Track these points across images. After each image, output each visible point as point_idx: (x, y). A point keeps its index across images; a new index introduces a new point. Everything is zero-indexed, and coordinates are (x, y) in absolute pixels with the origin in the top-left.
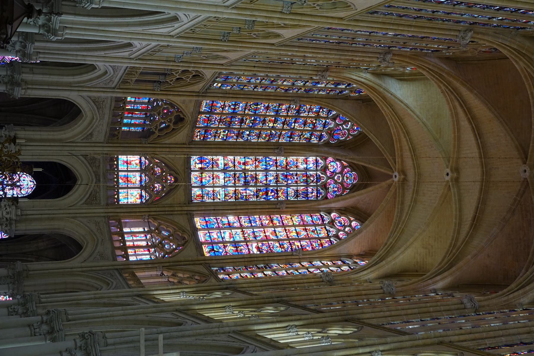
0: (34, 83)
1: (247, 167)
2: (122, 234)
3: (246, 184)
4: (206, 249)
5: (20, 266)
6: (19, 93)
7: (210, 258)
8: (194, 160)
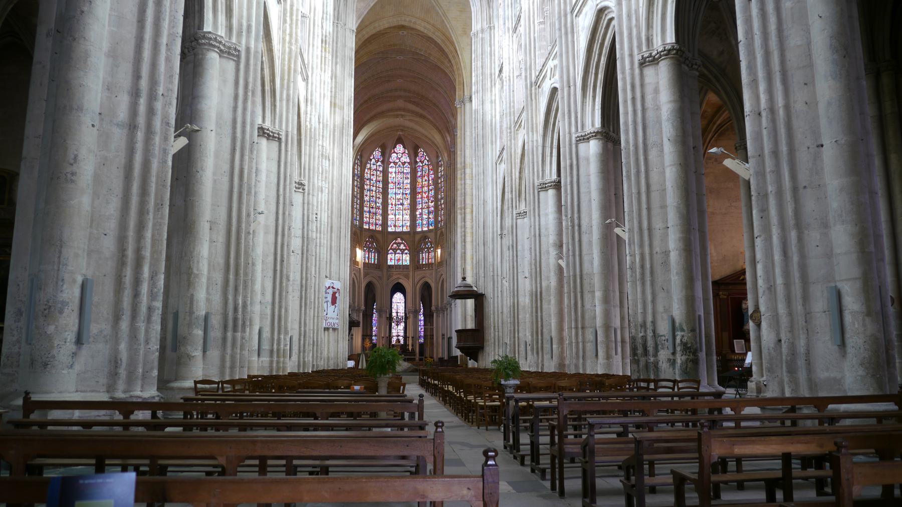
0: (358, 302)
1: (394, 203)
2: (422, 264)
3: (402, 204)
4: (431, 228)
5: (433, 308)
6: (363, 307)
7: (435, 227)
8: (390, 230)
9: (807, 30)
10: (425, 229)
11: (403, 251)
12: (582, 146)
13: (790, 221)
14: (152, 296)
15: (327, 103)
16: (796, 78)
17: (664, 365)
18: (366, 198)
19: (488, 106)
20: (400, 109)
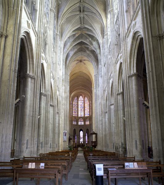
6: (73, 135)
9: (133, 98)
10: (87, 116)
11: (82, 121)
12: (111, 106)
13: (130, 129)
14: (36, 142)
15: (64, 93)
16: (132, 106)
17: (120, 151)
18: (73, 109)
19: (98, 91)
20: (81, 88)
